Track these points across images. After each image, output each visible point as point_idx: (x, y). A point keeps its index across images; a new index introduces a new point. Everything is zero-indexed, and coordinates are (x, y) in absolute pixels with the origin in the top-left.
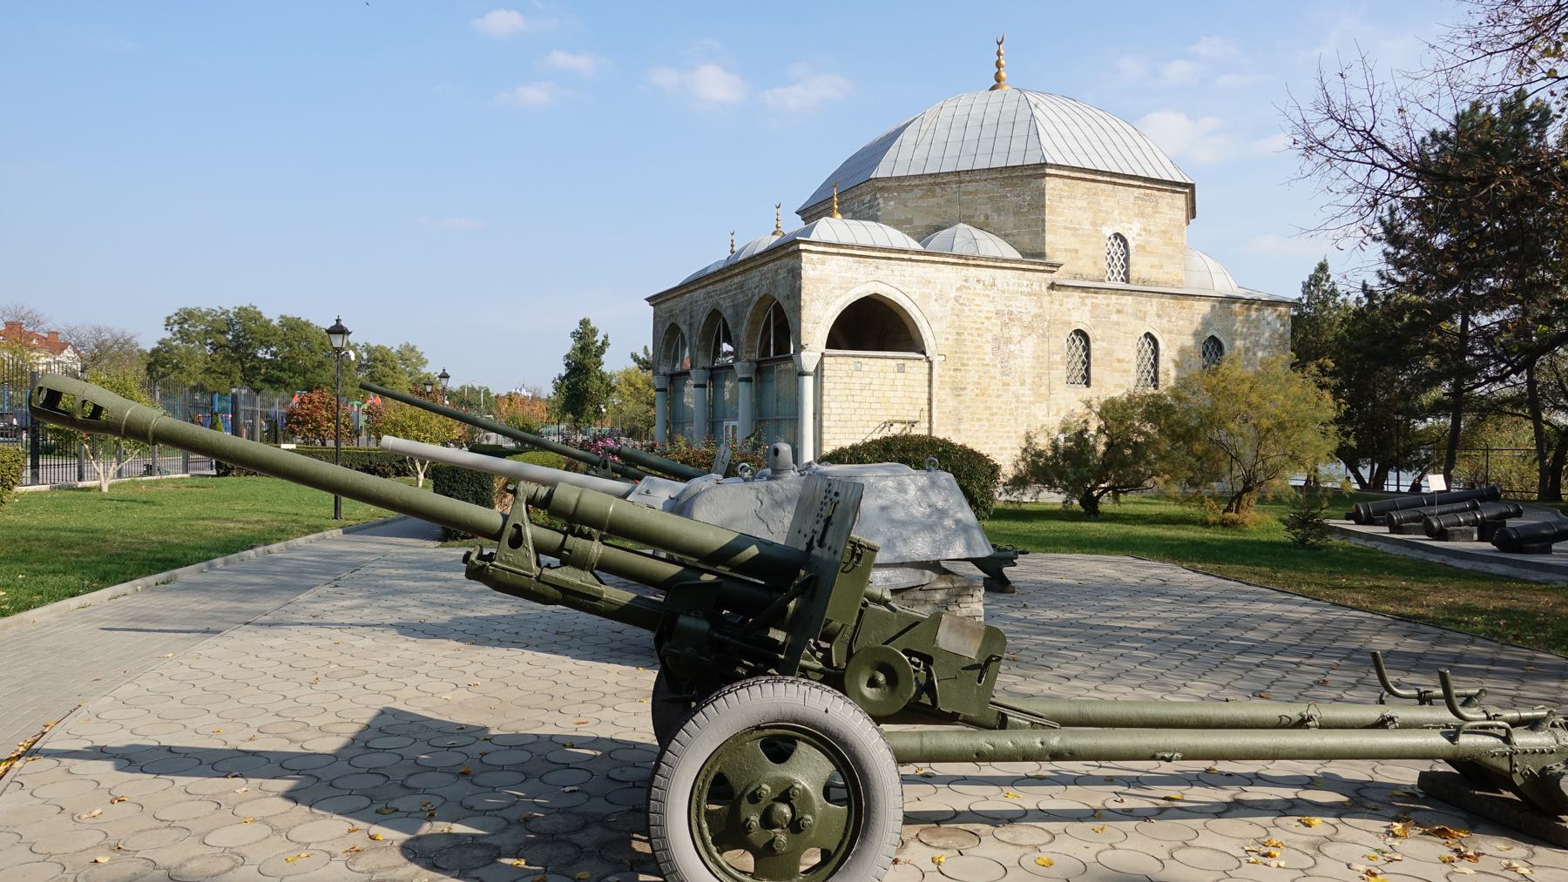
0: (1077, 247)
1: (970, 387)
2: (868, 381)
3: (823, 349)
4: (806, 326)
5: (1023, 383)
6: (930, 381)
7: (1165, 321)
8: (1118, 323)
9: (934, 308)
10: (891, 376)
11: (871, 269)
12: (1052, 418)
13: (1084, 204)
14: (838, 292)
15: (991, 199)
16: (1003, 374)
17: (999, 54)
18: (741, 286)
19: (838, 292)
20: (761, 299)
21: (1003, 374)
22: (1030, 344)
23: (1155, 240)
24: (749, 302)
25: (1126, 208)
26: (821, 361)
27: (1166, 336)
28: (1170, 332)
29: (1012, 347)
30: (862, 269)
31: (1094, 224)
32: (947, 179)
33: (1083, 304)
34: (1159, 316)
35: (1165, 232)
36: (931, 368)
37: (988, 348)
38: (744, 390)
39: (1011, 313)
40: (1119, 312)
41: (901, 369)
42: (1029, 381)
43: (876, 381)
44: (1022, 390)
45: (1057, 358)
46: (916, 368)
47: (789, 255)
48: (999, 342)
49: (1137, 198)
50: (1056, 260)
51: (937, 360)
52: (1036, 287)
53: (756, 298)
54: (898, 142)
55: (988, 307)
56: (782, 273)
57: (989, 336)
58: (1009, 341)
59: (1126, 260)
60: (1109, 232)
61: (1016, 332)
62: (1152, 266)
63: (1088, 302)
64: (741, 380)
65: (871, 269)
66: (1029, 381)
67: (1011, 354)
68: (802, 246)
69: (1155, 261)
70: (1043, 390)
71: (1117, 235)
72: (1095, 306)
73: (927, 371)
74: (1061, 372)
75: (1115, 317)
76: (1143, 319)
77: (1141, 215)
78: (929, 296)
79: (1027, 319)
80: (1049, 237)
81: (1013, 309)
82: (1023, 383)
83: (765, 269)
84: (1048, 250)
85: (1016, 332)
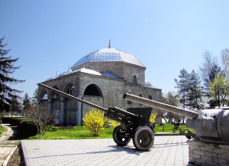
0: (128, 77)
3: (83, 95)
5: (120, 103)
6: (104, 102)
7: (143, 92)
8: (136, 92)
9: (104, 87)
10: (96, 101)
11: (93, 79)
13: (129, 69)
14: (86, 83)
15: (113, 67)
17: (110, 42)
19: (86, 83)
20: (68, 84)
21: (117, 101)
23: (141, 77)
24: (65, 85)
25: (136, 71)
26: (83, 97)
28: (144, 94)
29: (118, 96)
31: (131, 73)
33: (130, 88)
34: (142, 91)
35: (142, 76)
36: (104, 100)
37: (114, 96)
38: (62, 103)
39: (118, 89)
40: (136, 90)
41: (98, 100)
42: (121, 103)
44: (120, 105)
46: (101, 100)
47: (76, 75)
48: (116, 95)
50: (126, 79)
51: (105, 98)
53: (67, 84)
55: (114, 88)
56: (74, 79)
57: (114, 93)
58: (118, 94)
59: (136, 80)
60: (133, 75)
61: (119, 93)
63: (131, 88)
64: (62, 101)
65: (93, 79)
67: (118, 97)
68: (80, 73)
69: (141, 81)
70: (124, 104)
71: (135, 76)
72: (132, 88)
73: (103, 100)
75: (135, 91)
76: (140, 90)
77: (138, 72)
78: (103, 85)
79: (121, 90)
81: (118, 88)
83: (69, 78)
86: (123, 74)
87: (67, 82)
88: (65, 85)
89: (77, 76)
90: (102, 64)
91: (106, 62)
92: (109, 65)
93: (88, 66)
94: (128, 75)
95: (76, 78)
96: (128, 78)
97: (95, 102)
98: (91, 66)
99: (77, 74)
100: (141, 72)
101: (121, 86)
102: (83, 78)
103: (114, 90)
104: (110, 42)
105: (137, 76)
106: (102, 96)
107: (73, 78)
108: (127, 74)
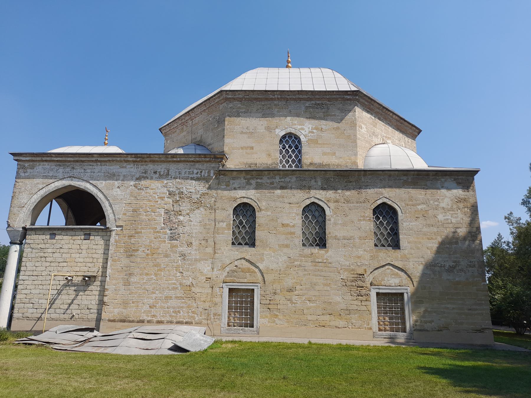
0: (253, 145)
1: (141, 249)
2: (59, 246)
5: (190, 244)
12: (216, 272)
16: (172, 238)
21: (172, 238)
22: (199, 215)
27: (332, 205)
28: (337, 201)
29: (181, 218)
30: (61, 170)
43: (65, 246)
45: (224, 225)
49: (307, 108)
52: (205, 174)
62: (324, 154)
65: (68, 170)
66: (195, 243)
67: (180, 223)
70: (210, 250)
74: (228, 235)
80: (227, 140)
81: (184, 190)
82: (190, 244)
84: (226, 149)
85: (185, 206)
86: (224, 137)
94: (249, 138)
96: (252, 148)
97: (74, 247)
100: (328, 116)
102: (29, 170)
103: (162, 198)
108: (242, 133)
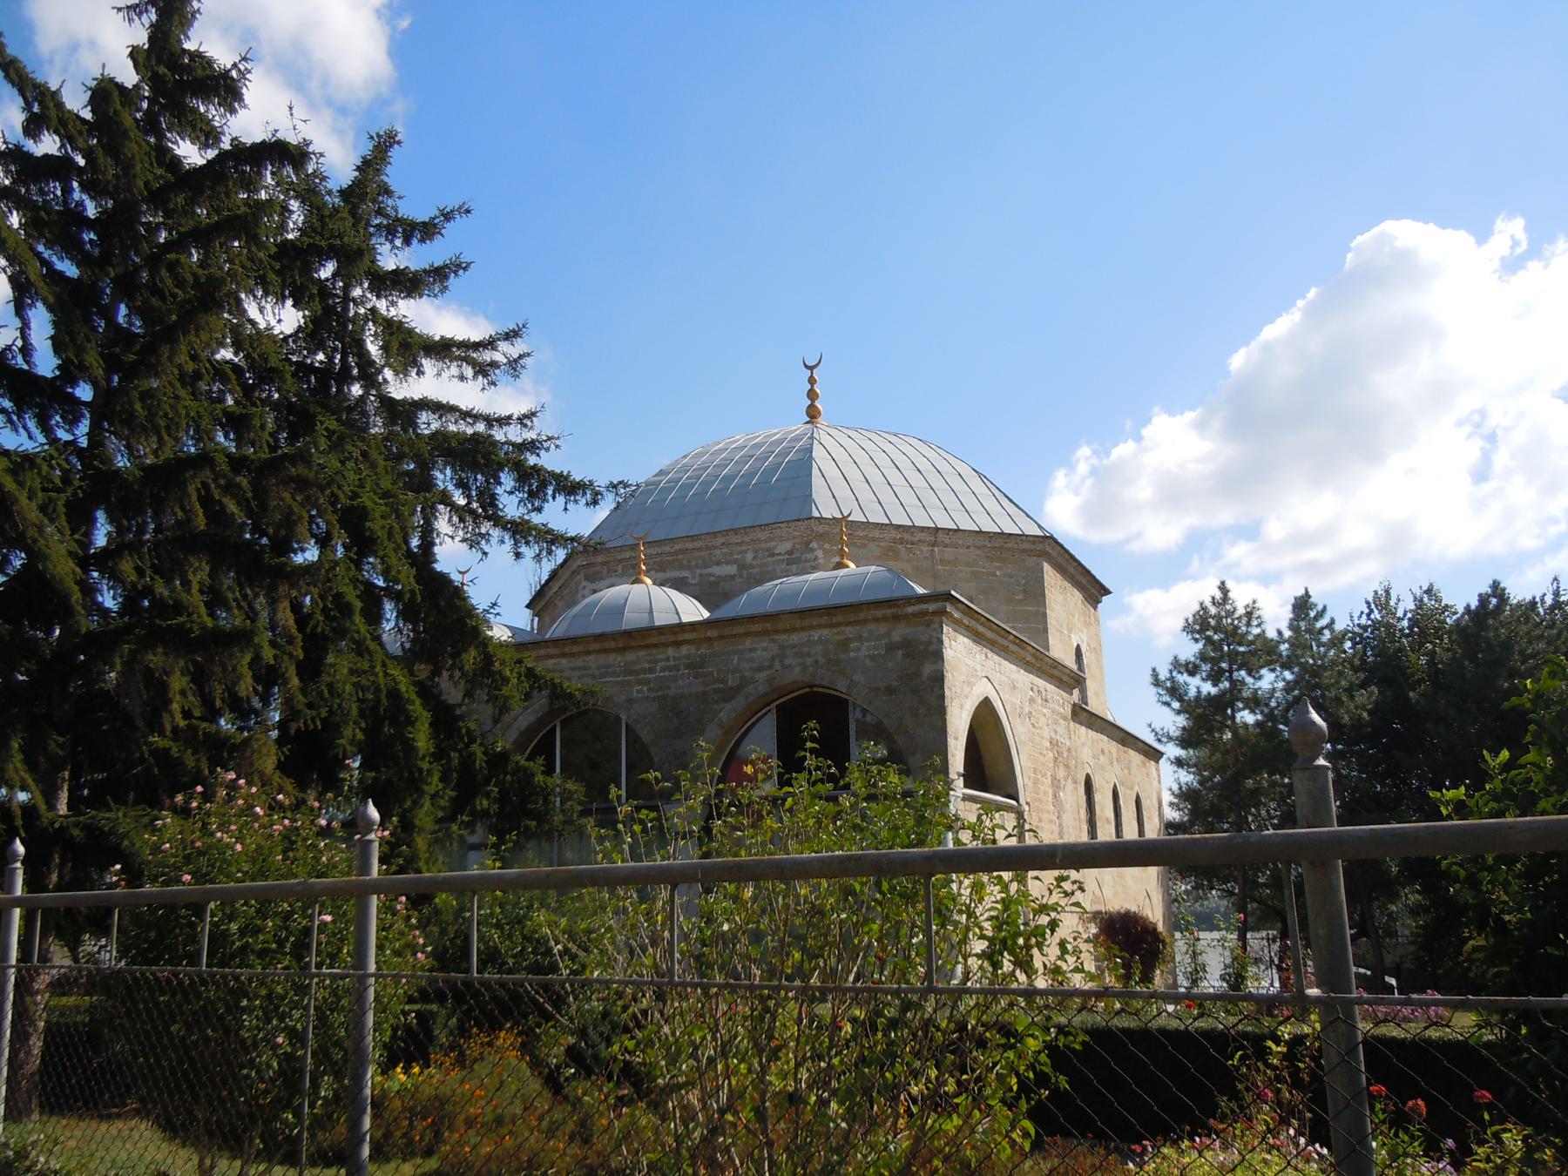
4: (951, 741)
17: (812, 381)
18: (695, 666)
32: (919, 536)
54: (815, 471)
87: (761, 669)
88: (728, 695)
89: (899, 632)
90: (901, 541)
91: (937, 529)
92: (949, 553)
93: (788, 546)
95: (891, 648)
98: (820, 553)
99: (910, 610)
101: (1065, 719)
104: (812, 381)
105: (1083, 649)
106: (1016, 799)
107: (844, 645)
